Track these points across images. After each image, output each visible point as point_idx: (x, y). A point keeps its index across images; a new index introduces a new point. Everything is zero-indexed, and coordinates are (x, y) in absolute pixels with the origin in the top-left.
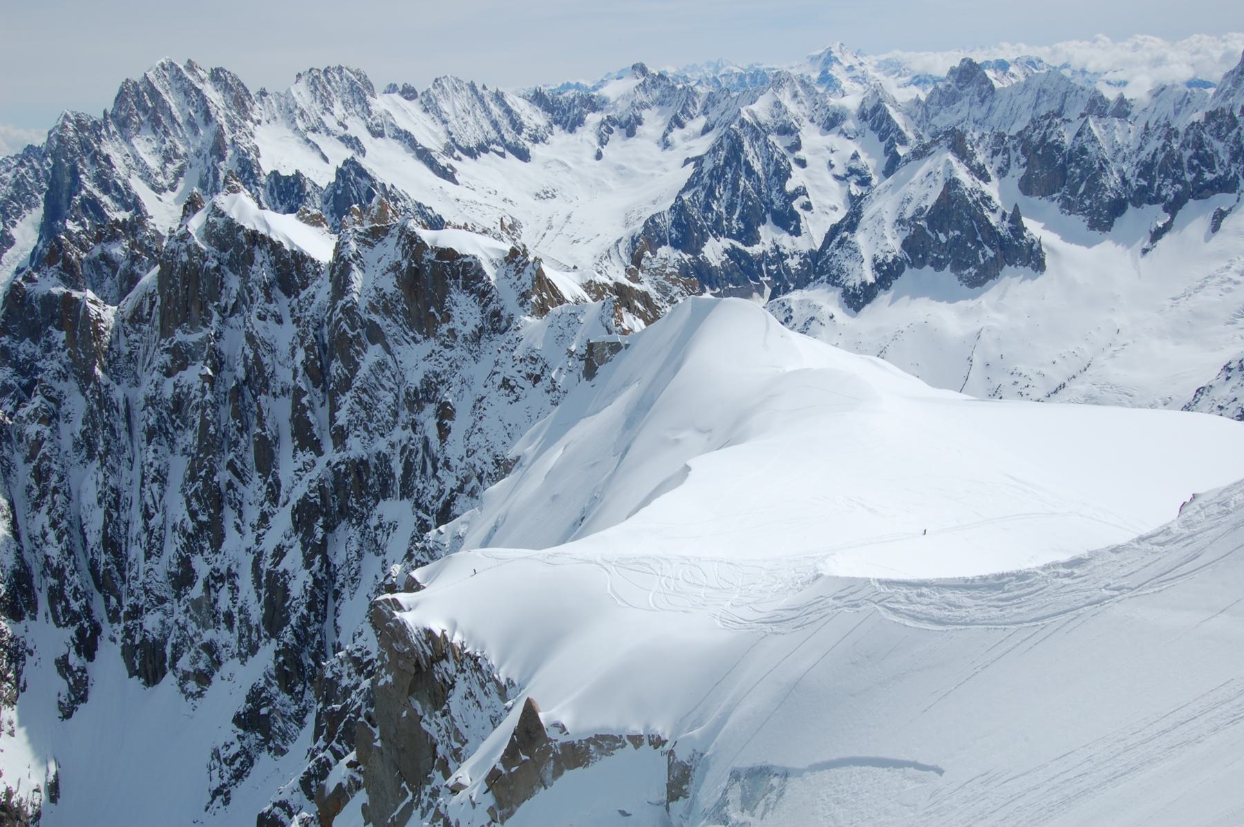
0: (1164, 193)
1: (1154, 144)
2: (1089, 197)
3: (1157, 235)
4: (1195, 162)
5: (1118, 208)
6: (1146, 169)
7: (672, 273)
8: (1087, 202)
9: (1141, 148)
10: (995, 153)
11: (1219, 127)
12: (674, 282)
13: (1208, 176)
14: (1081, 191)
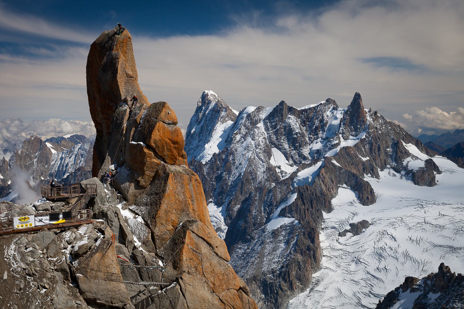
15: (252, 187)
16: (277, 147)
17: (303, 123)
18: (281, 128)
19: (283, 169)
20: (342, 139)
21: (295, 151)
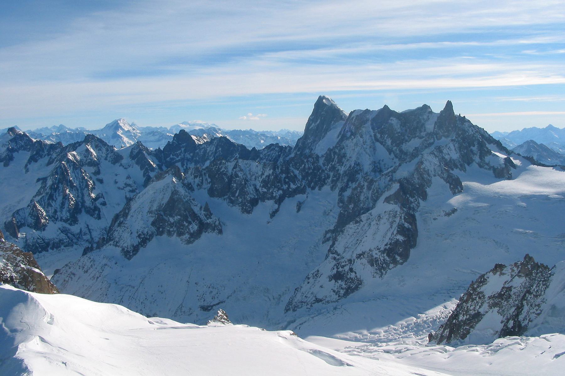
0: (274, 195)
1: (269, 172)
2: (241, 198)
3: (274, 214)
4: (287, 180)
5: (254, 202)
6: (265, 183)
7: (17, 250)
8: (240, 200)
9: (263, 174)
10: (196, 177)
11: (296, 164)
12: (18, 255)
13: (293, 186)
14: (237, 194)
15: (359, 176)
21: (396, 148)
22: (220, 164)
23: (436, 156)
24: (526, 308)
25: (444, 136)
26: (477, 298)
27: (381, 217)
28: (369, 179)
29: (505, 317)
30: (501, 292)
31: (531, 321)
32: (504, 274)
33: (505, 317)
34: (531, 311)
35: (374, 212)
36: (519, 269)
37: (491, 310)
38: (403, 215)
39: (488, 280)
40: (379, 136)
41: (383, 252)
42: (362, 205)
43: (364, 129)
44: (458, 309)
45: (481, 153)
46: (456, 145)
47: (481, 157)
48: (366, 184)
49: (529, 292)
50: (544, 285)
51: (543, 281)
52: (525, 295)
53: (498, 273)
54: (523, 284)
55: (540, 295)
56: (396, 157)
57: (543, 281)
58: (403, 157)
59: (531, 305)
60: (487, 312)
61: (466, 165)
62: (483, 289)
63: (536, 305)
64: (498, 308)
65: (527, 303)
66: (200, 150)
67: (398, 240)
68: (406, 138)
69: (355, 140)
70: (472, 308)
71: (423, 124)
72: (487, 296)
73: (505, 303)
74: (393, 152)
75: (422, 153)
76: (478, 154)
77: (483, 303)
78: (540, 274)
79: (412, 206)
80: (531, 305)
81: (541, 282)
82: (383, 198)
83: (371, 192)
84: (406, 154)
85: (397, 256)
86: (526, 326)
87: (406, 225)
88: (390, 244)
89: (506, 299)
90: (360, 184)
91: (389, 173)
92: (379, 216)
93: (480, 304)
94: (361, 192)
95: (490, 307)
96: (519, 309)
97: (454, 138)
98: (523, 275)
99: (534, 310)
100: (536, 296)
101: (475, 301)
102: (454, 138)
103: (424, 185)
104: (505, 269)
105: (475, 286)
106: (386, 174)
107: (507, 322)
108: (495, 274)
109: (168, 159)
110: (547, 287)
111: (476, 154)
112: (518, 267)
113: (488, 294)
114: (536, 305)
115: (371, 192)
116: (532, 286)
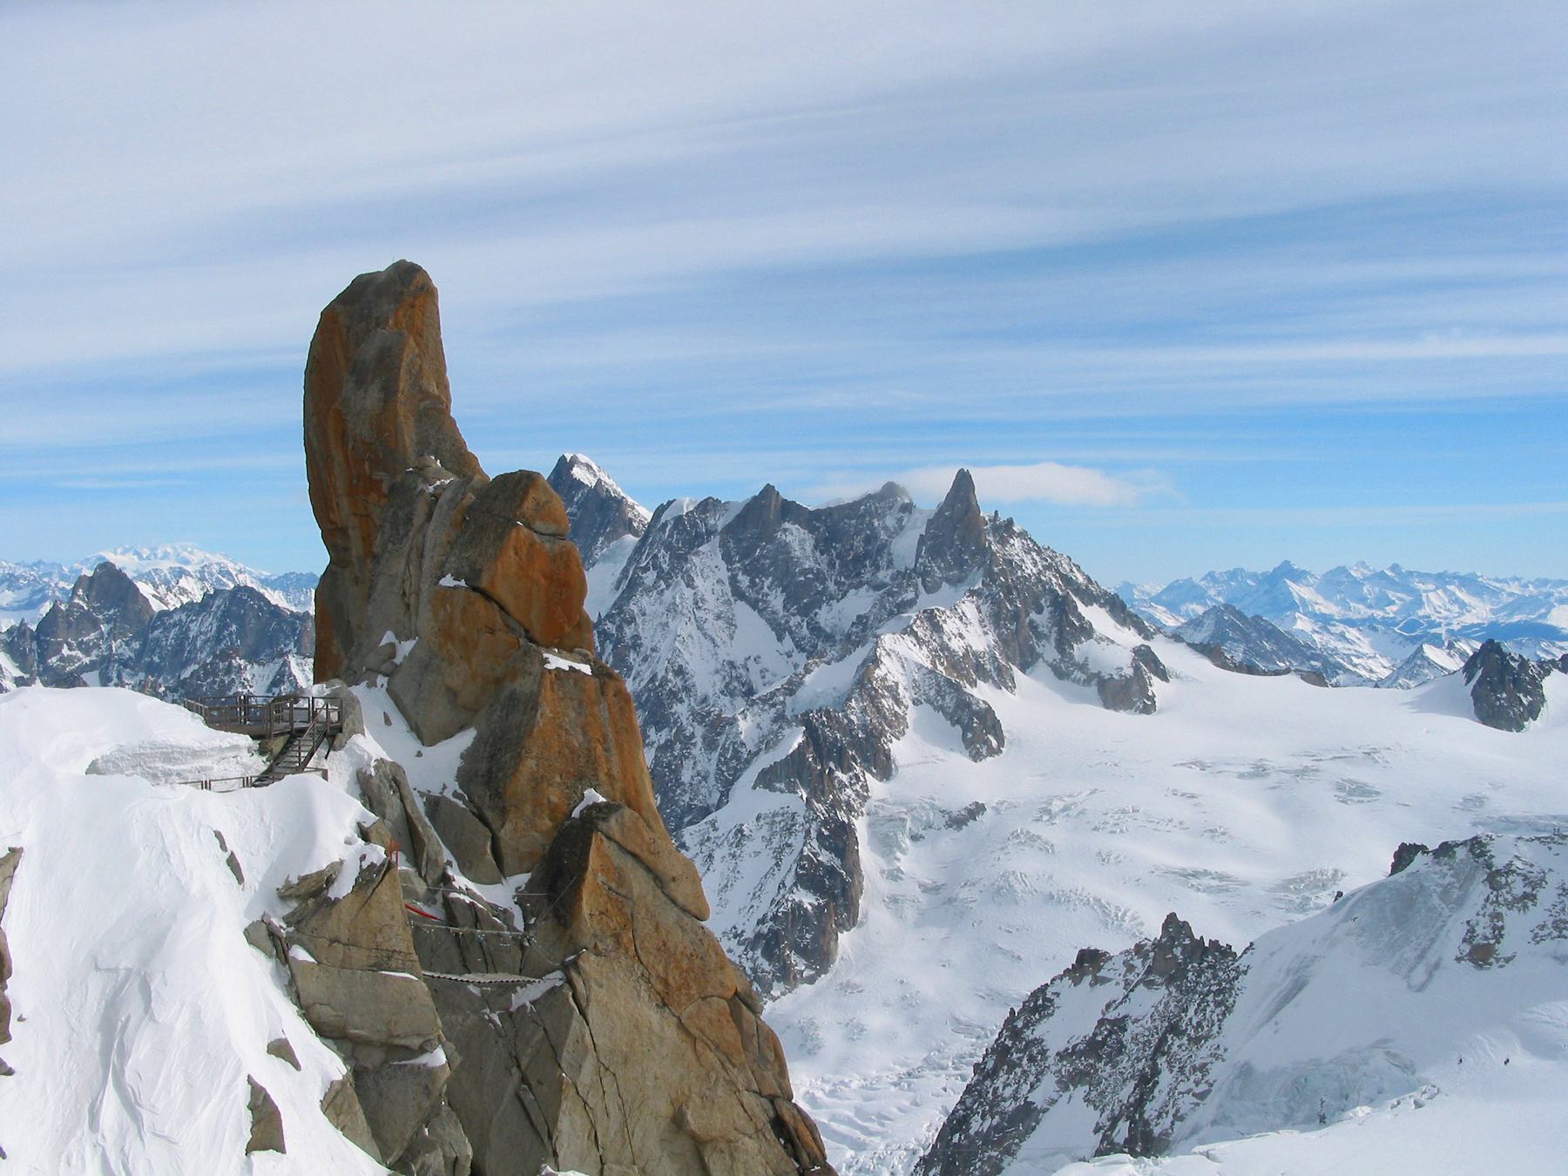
15: (681, 710)
16: (754, 605)
17: (823, 545)
18: (762, 556)
19: (766, 662)
20: (921, 587)
21: (798, 618)
22: (228, 671)
23: (920, 642)
24: (1166, 1078)
25: (948, 581)
26: (1025, 1061)
27: (746, 832)
28: (709, 713)
29: (1107, 1112)
30: (1095, 1035)
31: (1182, 1119)
32: (1104, 980)
33: (1107, 1112)
34: (1182, 1087)
35: (725, 818)
36: (1149, 962)
37: (1067, 1094)
38: (814, 825)
39: (1057, 1001)
40: (744, 580)
41: (752, 944)
42: (686, 798)
43: (695, 559)
44: (969, 1101)
45: (1061, 632)
46: (984, 608)
47: (1063, 645)
48: (699, 731)
49: (1174, 1029)
50: (1218, 1004)
51: (1217, 993)
52: (1163, 1040)
53: (1088, 979)
54: (1161, 1008)
55: (1206, 1038)
56: (801, 649)
57: (1217, 993)
58: (818, 642)
59: (1181, 1070)
60: (1053, 1102)
61: (1016, 671)
62: (1042, 1030)
63: (1194, 1069)
64: (1087, 1088)
65: (1169, 1063)
66: (167, 629)
67: (799, 906)
68: (832, 587)
69: (668, 595)
70: (1008, 1092)
71: (884, 546)
72: (1052, 1053)
73: (1108, 1068)
74: (791, 633)
75: (878, 632)
76: (1054, 636)
77: (1041, 1073)
78: (1209, 974)
79: (843, 797)
80: (1181, 1070)
81: (1210, 998)
82: (751, 774)
83: (715, 755)
84: (829, 638)
85: (794, 958)
86: (1165, 1133)
87: (825, 857)
88: (775, 918)
89: (1109, 1055)
90: (681, 730)
91: (773, 694)
92: (740, 831)
93: (1032, 1078)
94: (684, 757)
95: (1065, 1083)
96: (1146, 1082)
97: (979, 586)
98: (1160, 981)
99: (1191, 1084)
100: (1196, 1041)
101: (1018, 1070)
102: (979, 586)
103: (882, 733)
104: (1108, 965)
105: (1020, 1024)
106: (764, 700)
107: (1113, 1127)
108: (1076, 982)
109: (53, 660)
110: (1229, 1010)
111: (1046, 637)
112: (1146, 957)
113: (1055, 1044)
114: (1194, 1069)
115: (715, 755)
116: (1185, 1010)
